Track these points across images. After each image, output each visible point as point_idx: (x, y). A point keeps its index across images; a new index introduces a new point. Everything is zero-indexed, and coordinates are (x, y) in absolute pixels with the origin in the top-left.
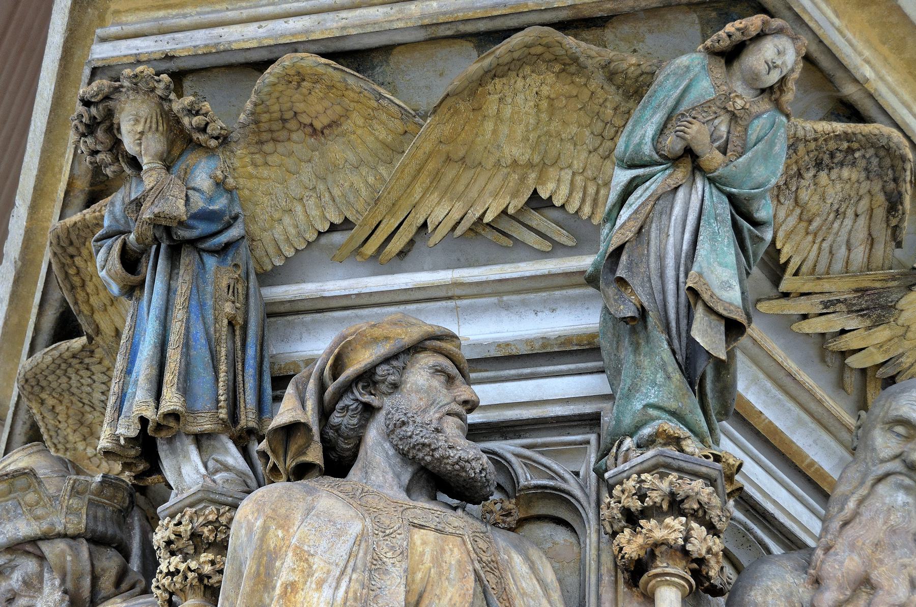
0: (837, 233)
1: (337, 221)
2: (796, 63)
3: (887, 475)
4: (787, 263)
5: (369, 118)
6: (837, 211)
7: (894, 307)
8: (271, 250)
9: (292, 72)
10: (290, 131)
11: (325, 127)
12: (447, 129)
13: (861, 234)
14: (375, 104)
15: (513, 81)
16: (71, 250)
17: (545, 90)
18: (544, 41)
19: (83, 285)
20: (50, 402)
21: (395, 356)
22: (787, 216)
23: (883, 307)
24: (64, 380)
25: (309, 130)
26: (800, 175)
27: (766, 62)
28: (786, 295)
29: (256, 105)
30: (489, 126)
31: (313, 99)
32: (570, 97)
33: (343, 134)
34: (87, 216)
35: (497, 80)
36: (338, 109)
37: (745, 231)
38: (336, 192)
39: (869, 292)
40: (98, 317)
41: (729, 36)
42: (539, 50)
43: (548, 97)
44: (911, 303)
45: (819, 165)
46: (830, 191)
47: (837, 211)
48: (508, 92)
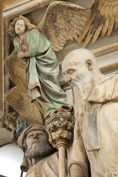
0: (75, 23)
2: (24, 20)
4: (74, 39)
5: (20, 91)
6: (67, 22)
7: (102, 17)
8: (39, 120)
9: (6, 99)
10: (22, 102)
11: (21, 97)
12: (22, 85)
13: (79, 17)
15: (15, 69)
17: (19, 64)
18: (6, 62)
21: (23, 141)
22: (64, 33)
23: (101, 19)
26: (56, 26)
27: (17, 30)
28: (84, 40)
31: (15, 97)
33: (23, 96)
35: (14, 72)
37: (41, 59)
39: (94, 21)
42: (8, 64)
43: (21, 64)
44: (103, 12)
45: (55, 21)
46: (61, 22)
47: (67, 22)
48: (17, 71)
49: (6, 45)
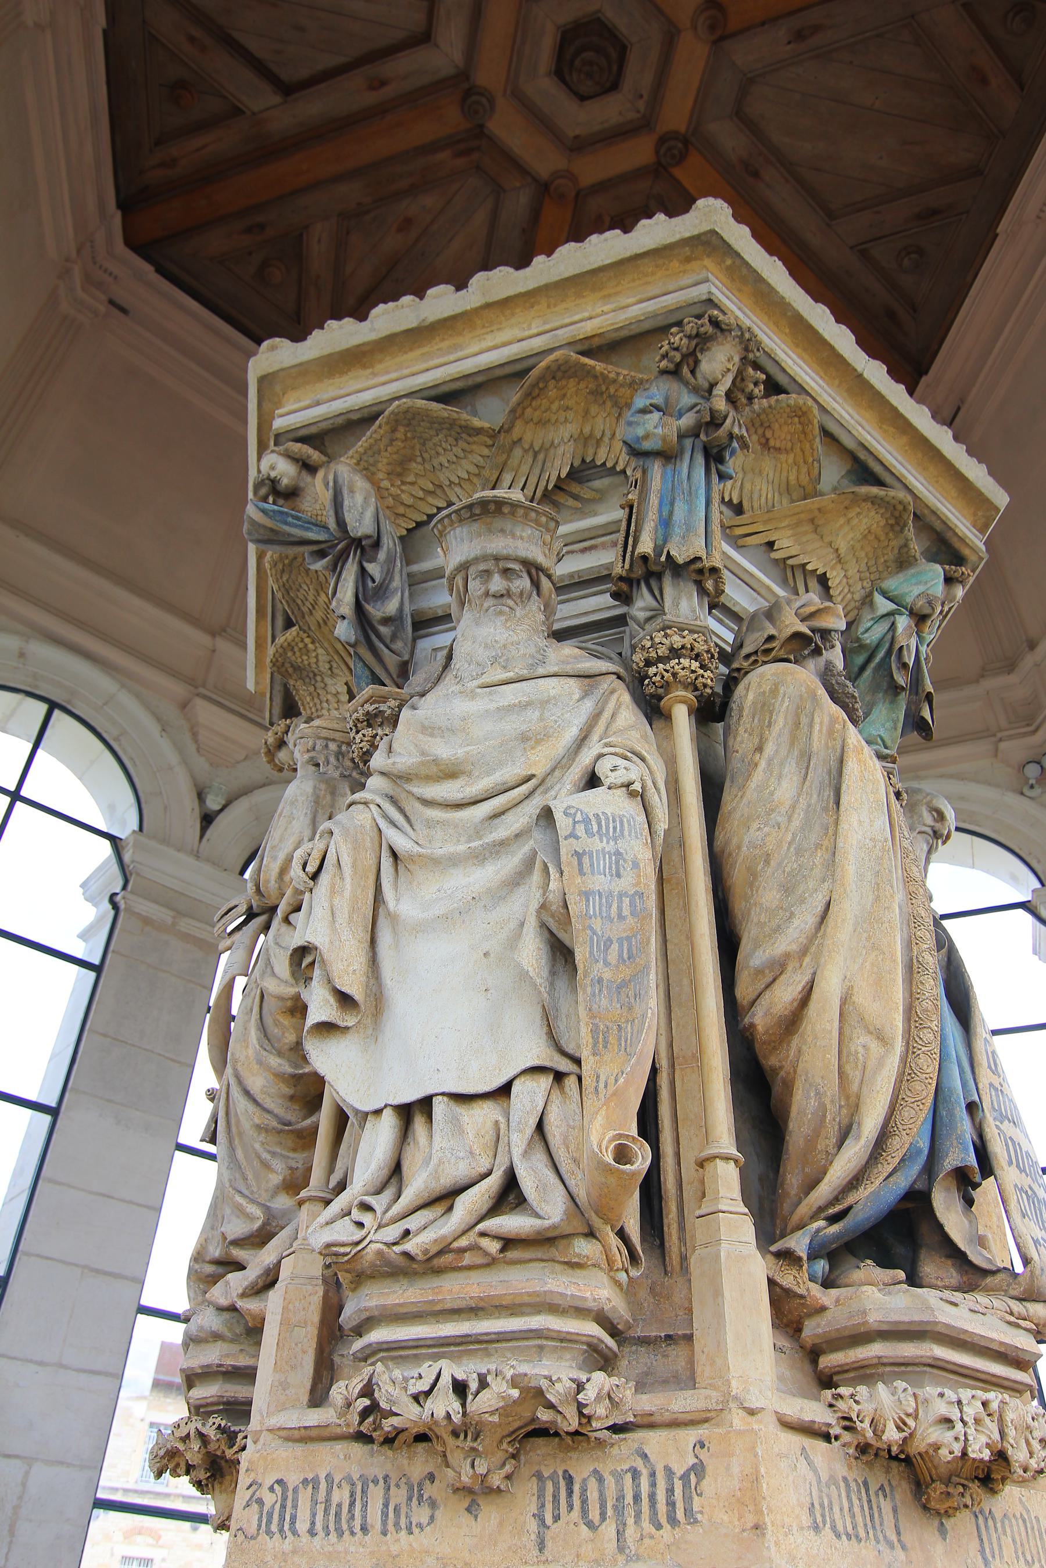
1: (735, 501)
3: (923, 832)
10: (756, 432)
11: (775, 448)
14: (811, 460)
16: (559, 374)
19: (533, 398)
20: (399, 435)
24: (432, 432)
25: (763, 441)
29: (770, 407)
30: (842, 520)
31: (785, 429)
32: (877, 538)
34: (598, 368)
36: (789, 445)
38: (748, 486)
40: (519, 424)
41: (963, 573)
49: (926, 512)
